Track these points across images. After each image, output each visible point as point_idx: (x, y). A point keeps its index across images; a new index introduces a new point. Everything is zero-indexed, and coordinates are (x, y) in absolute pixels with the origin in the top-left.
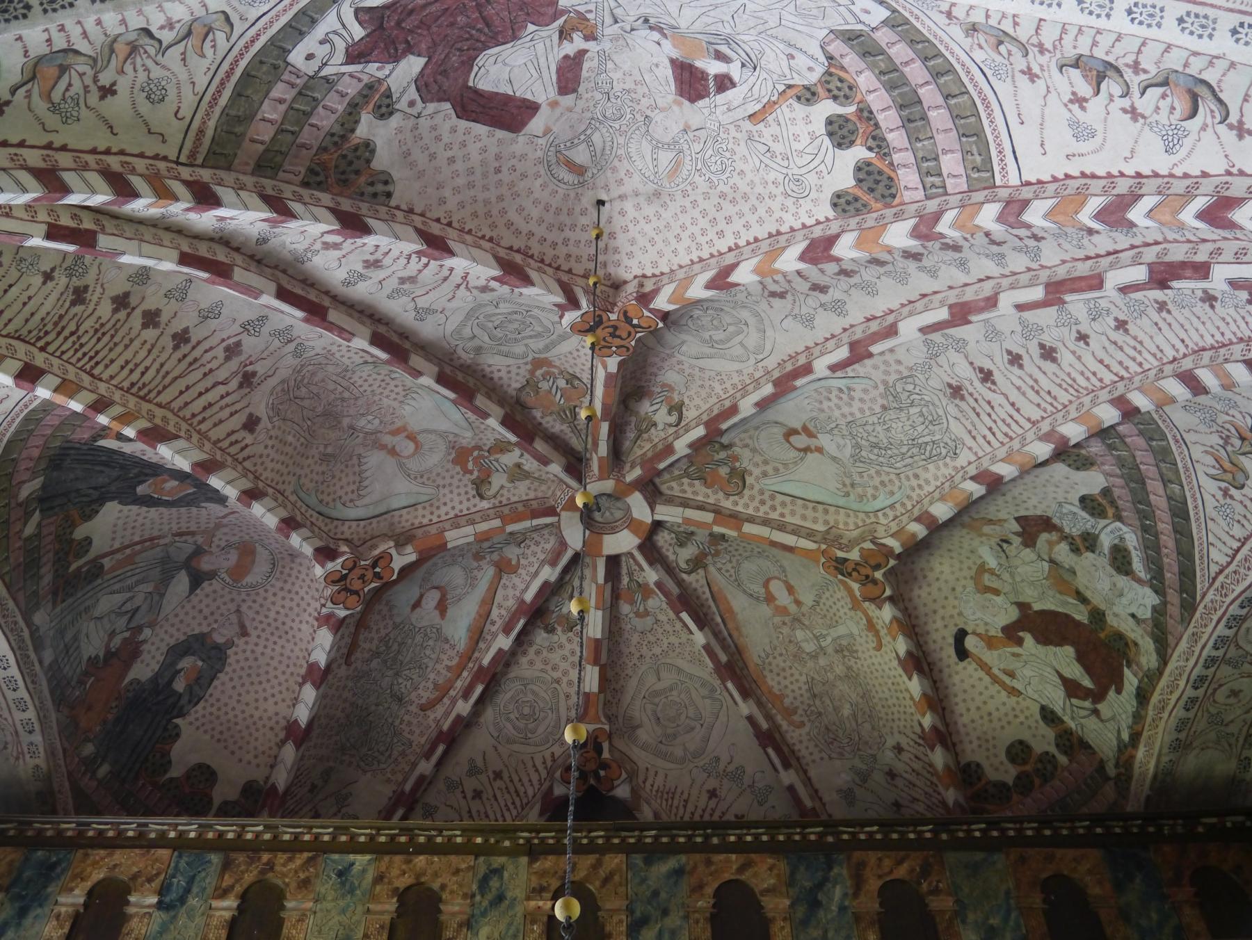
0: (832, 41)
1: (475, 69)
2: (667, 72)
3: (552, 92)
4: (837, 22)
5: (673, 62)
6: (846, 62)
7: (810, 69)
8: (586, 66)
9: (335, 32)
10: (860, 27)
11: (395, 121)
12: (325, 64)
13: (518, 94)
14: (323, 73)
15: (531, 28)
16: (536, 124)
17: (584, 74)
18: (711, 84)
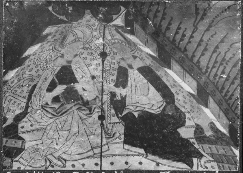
0: (22, 146)
1: (161, 109)
2: (78, 75)
3: (130, 71)
4: (24, 154)
5: (75, 81)
6: (13, 141)
7: (23, 127)
8: (114, 78)
9: (202, 167)
10: (17, 159)
11: (199, 122)
12: (210, 161)
13: (146, 81)
14: (212, 159)
15: (136, 114)
16: (141, 64)
17: (116, 73)
18: (57, 81)
